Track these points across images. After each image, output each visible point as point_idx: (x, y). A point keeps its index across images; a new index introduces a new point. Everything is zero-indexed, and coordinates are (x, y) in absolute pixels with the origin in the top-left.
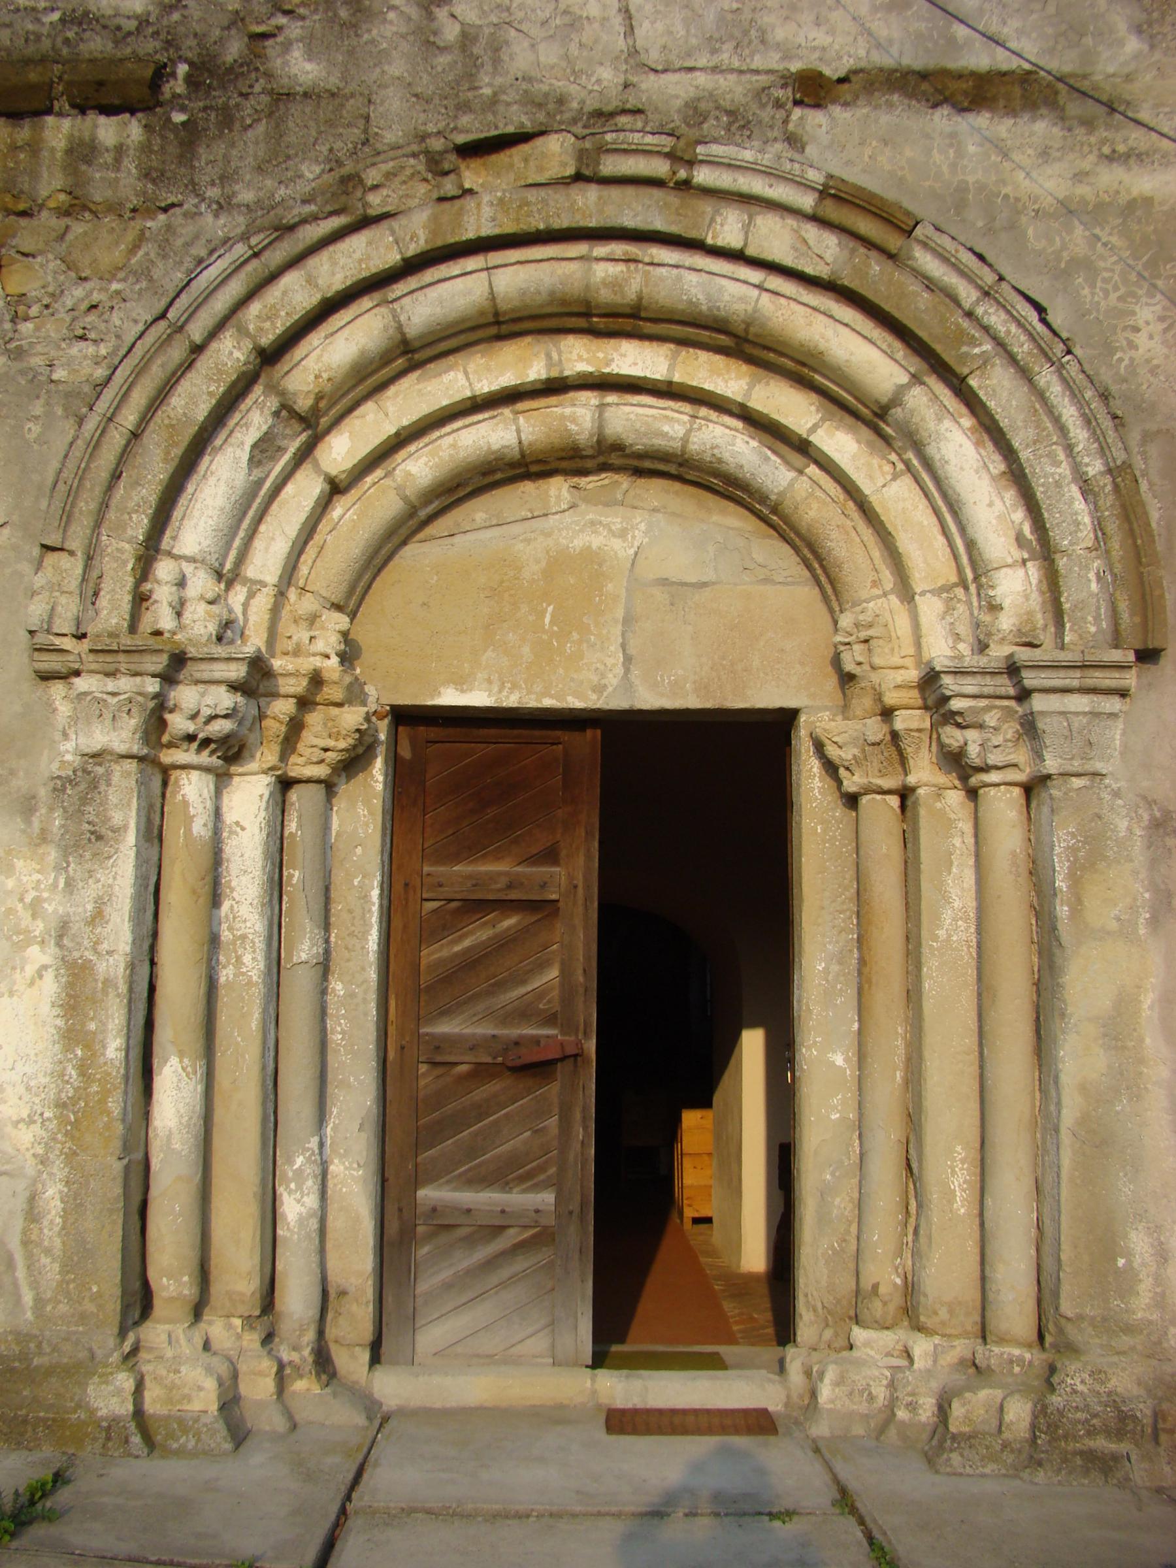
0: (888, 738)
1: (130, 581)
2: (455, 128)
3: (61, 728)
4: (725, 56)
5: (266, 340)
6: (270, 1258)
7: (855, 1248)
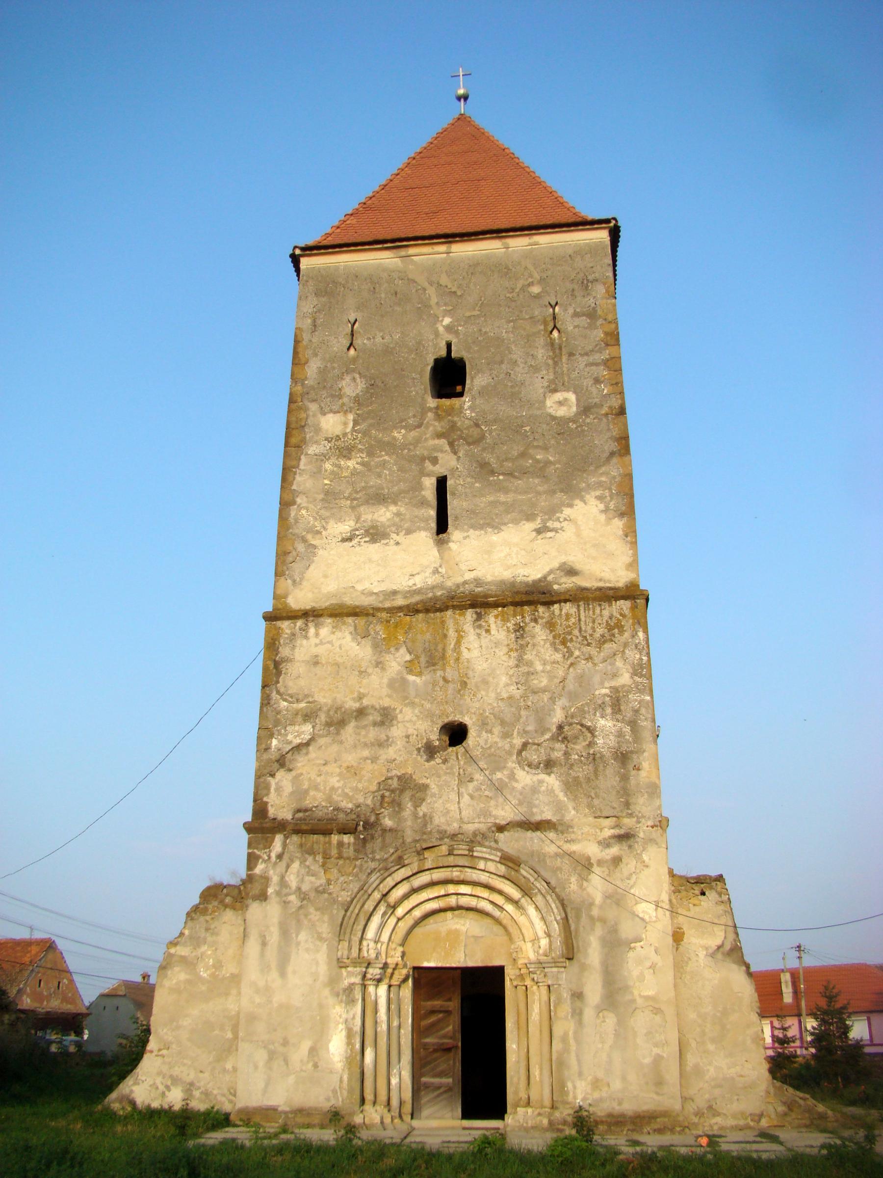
4: (482, 820)
5: (384, 893)
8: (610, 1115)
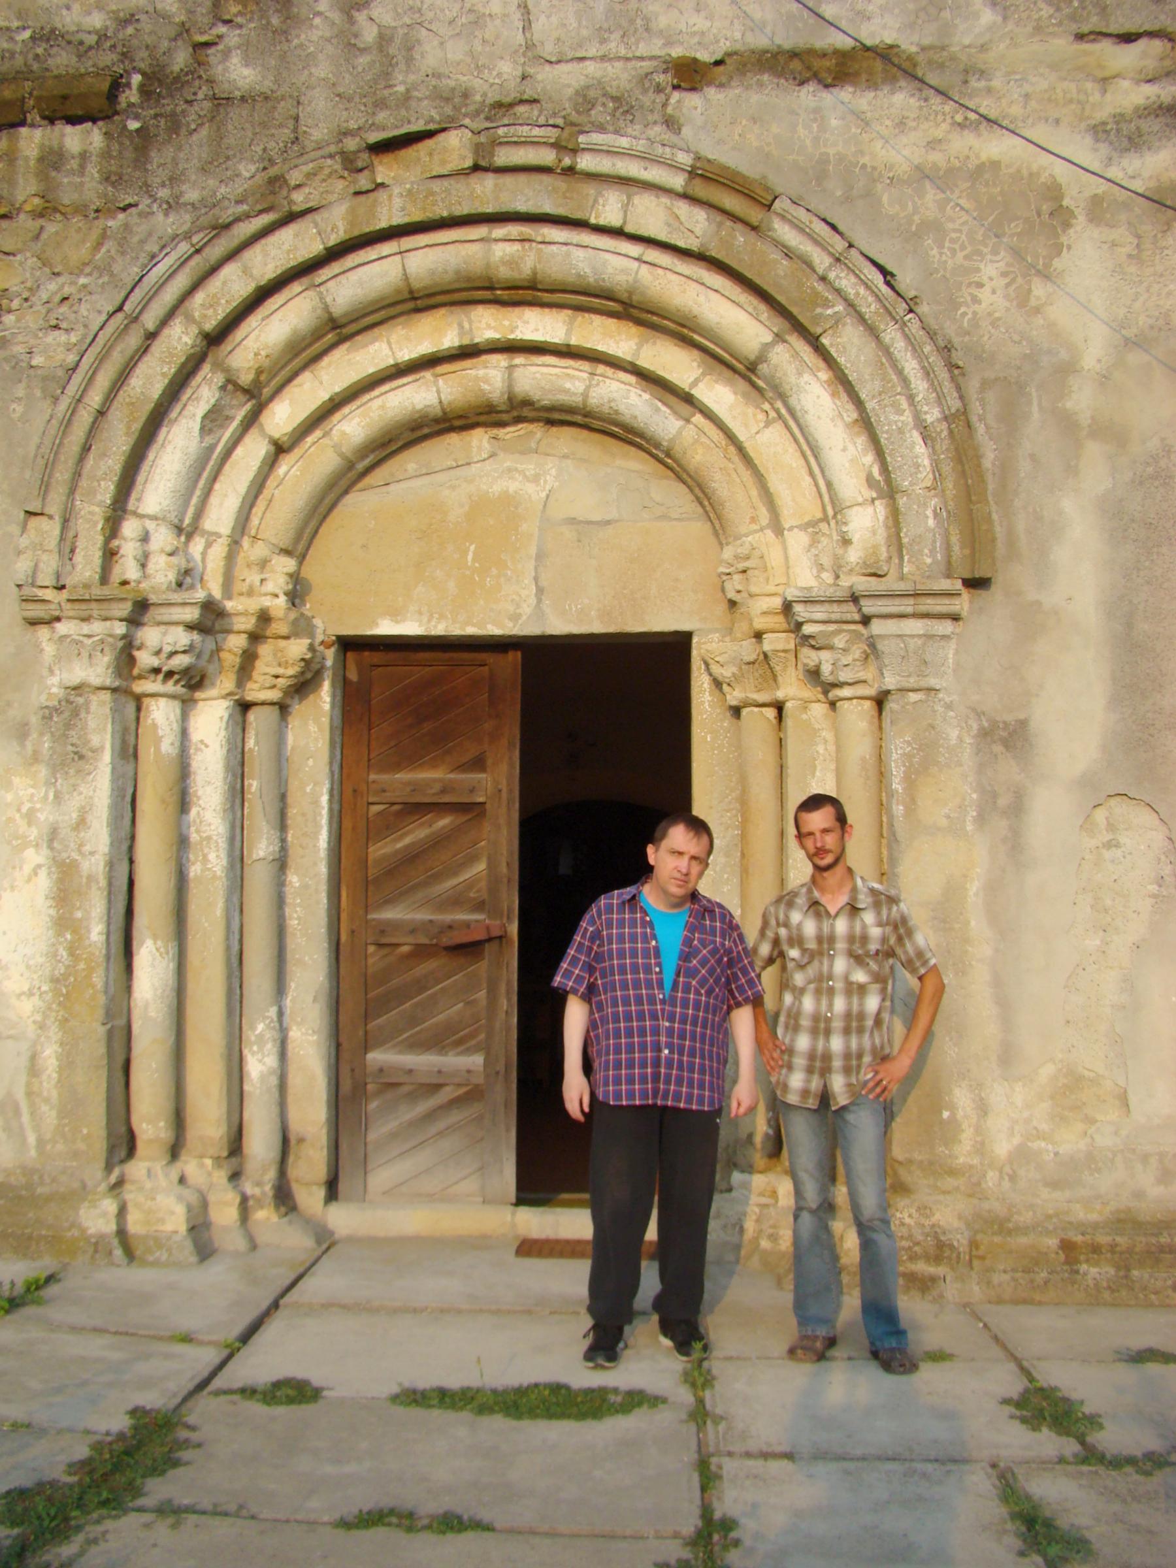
1: (100, 540)
2: (373, 124)
3: (47, 665)
4: (614, 46)
5: (210, 326)
8: (1124, 1221)
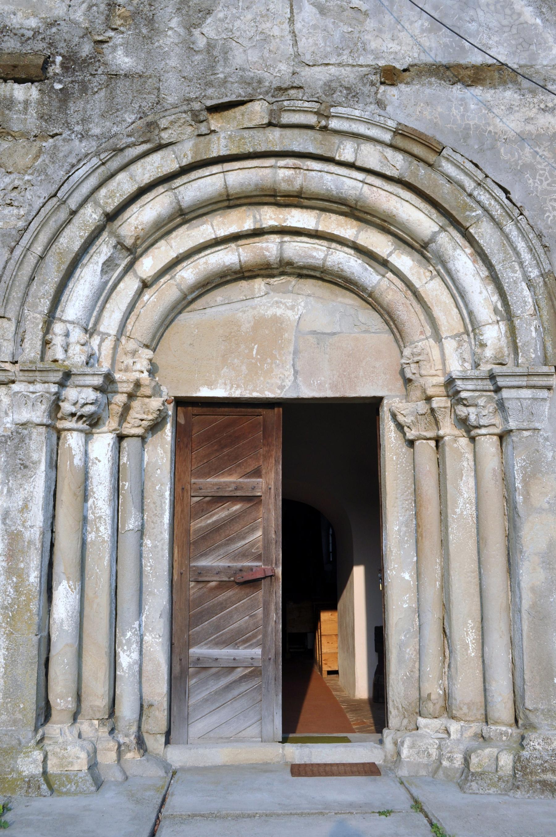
0: (429, 411)
1: (41, 334)
2: (205, 96)
3: (4, 410)
4: (345, 58)
6: (113, 687)
7: (417, 675)
